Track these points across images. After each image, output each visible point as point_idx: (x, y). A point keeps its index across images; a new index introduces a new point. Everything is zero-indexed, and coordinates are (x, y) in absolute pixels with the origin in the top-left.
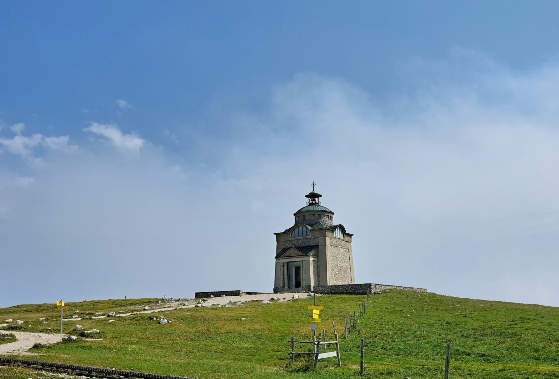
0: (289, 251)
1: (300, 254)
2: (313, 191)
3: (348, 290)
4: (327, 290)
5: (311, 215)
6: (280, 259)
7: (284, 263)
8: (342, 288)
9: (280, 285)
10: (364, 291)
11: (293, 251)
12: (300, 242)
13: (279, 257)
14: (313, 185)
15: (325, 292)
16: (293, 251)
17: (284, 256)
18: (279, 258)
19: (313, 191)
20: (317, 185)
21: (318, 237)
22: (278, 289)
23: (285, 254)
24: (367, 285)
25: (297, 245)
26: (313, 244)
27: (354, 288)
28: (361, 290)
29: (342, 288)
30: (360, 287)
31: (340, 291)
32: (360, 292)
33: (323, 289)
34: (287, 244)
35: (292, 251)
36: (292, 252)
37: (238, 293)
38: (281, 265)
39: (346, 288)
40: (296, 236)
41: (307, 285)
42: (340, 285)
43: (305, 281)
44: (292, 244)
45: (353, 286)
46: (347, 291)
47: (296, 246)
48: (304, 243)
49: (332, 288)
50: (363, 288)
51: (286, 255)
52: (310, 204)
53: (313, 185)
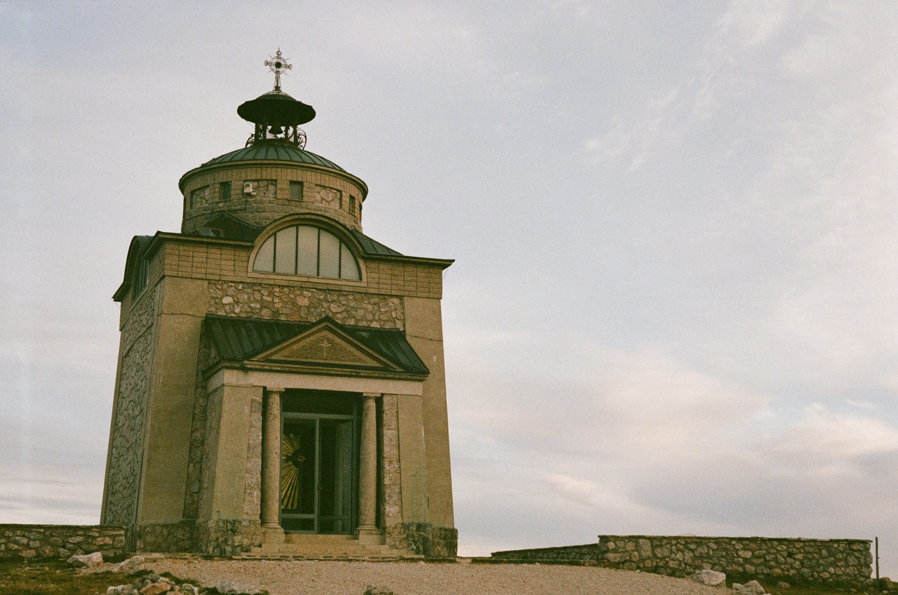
0: (309, 336)
1: (357, 353)
2: (277, 88)
3: (773, 563)
4: (679, 556)
5: (325, 187)
6: (245, 370)
7: (267, 393)
8: (749, 555)
9: (246, 508)
10: (844, 574)
11: (329, 341)
12: (303, 302)
13: (248, 357)
14: (278, 65)
15: (666, 565)
16: (329, 341)
17: (274, 358)
18: (248, 364)
19: (277, 88)
20: (294, 68)
21: (402, 293)
22: (234, 532)
23: (279, 351)
24: (855, 547)
25: (285, 311)
26: (375, 325)
27: (800, 556)
28: (832, 570)
29: (749, 555)
30: (824, 552)
31: (741, 569)
32: (826, 575)
33: (659, 552)
34: (227, 300)
35: (324, 340)
36: (325, 345)
37: (108, 540)
38: (253, 401)
39: (768, 553)
40: (278, 270)
41: (406, 521)
42: (740, 540)
43: (395, 498)
44: (256, 301)
45: (798, 545)
46: (771, 568)
47: (283, 318)
48: (329, 308)
49: (703, 550)
50: (840, 560)
51: (286, 352)
52: (258, 142)
53: (278, 65)
